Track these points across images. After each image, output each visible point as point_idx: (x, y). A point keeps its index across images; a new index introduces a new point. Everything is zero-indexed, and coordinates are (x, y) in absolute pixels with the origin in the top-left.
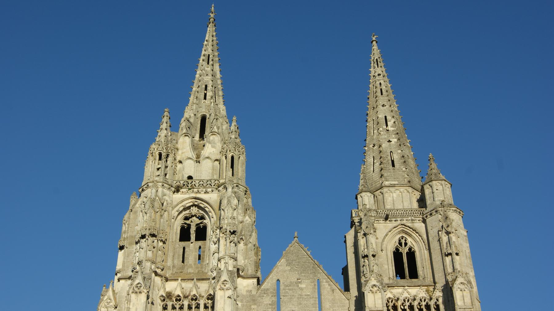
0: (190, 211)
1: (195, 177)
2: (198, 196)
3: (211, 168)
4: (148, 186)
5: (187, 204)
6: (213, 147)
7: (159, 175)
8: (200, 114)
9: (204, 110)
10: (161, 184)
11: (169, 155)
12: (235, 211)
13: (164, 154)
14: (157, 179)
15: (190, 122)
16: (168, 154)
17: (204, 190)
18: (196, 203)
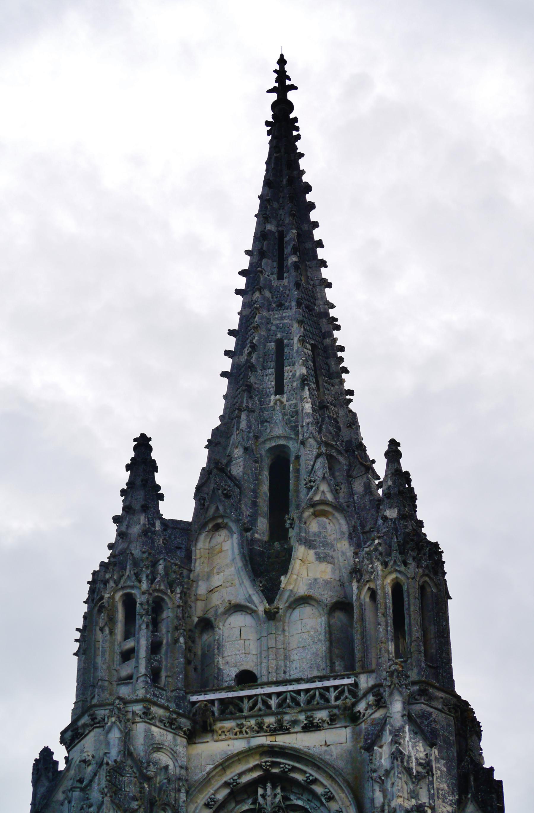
0: (255, 802)
1: (264, 672)
2: (281, 740)
3: (322, 637)
4: (93, 718)
5: (240, 775)
6: (321, 558)
7: (130, 677)
8: (268, 446)
9: (278, 430)
10: (138, 708)
11: (163, 600)
12: (424, 785)
13: (144, 598)
14: (124, 691)
15: (231, 477)
16: (158, 596)
17: (302, 717)
18: (275, 770)
